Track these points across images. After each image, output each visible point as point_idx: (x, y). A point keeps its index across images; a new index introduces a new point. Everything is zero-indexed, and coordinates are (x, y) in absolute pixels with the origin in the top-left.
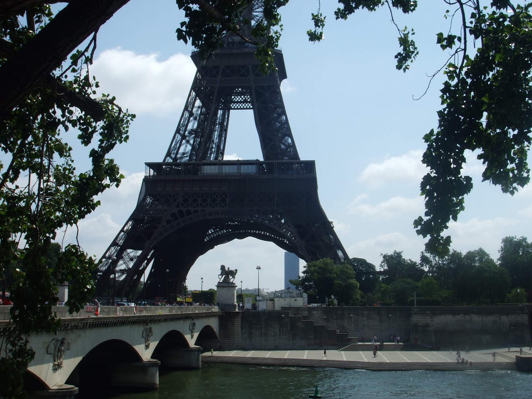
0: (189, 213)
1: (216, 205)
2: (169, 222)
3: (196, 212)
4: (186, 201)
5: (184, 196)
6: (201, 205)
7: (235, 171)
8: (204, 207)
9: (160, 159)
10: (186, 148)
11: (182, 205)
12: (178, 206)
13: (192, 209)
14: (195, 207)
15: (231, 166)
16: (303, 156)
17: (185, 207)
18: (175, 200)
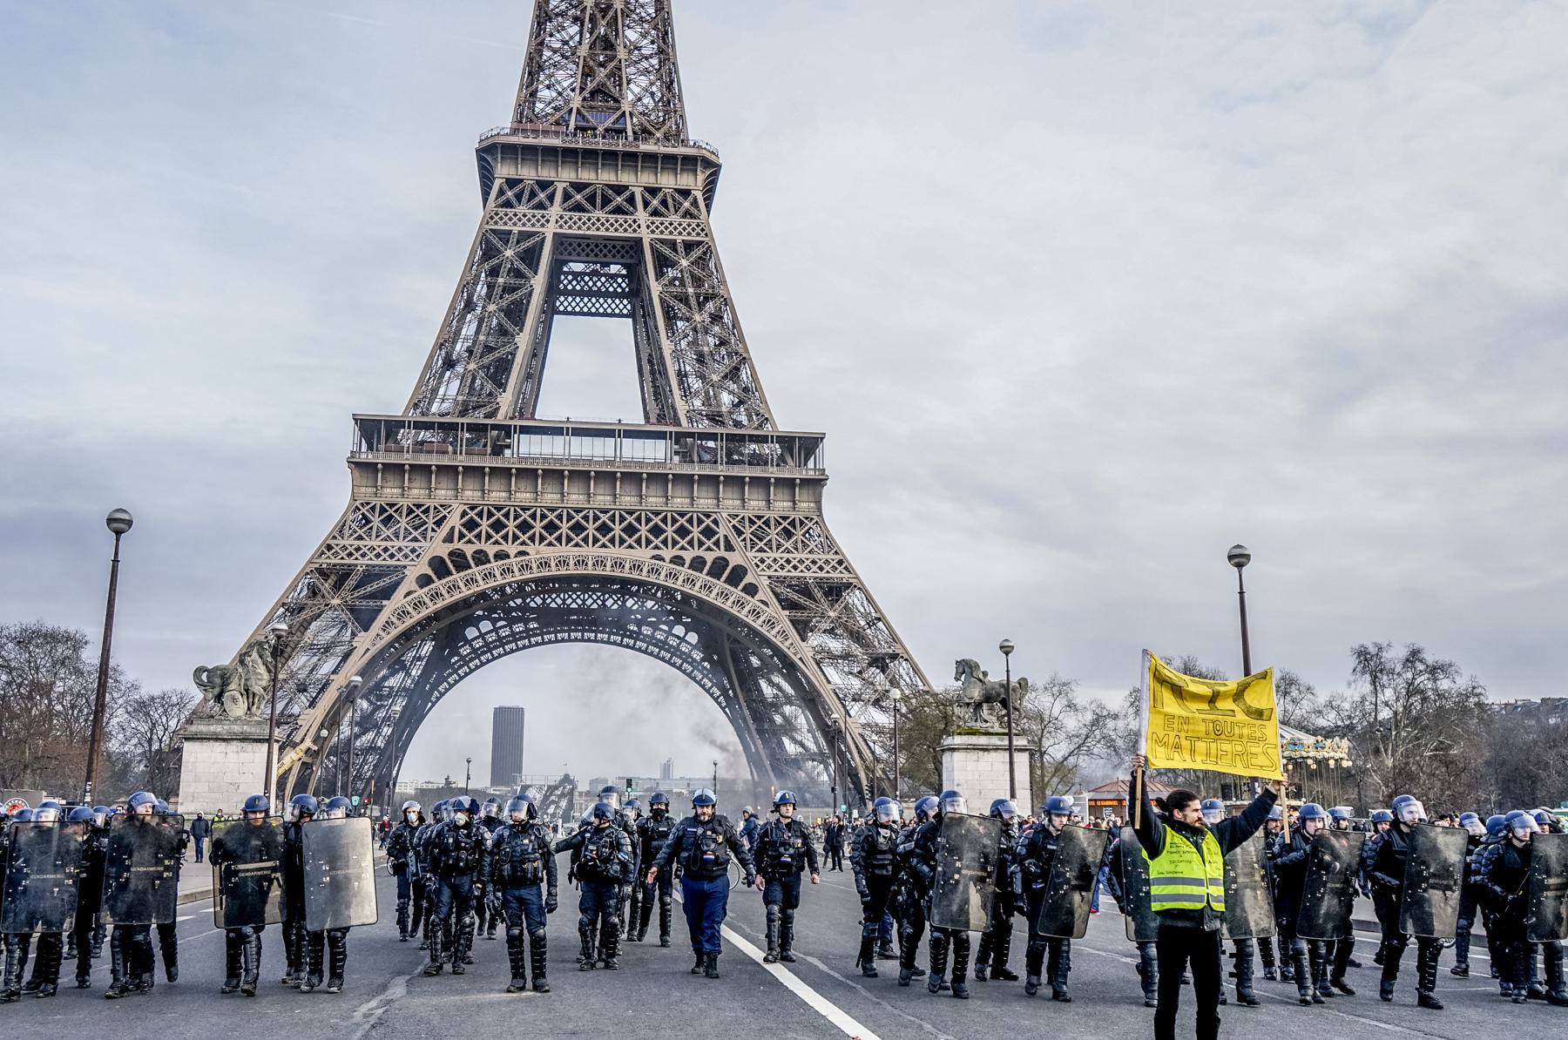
0: (481, 558)
1: (559, 539)
2: (424, 581)
3: (501, 556)
4: (471, 525)
5: (464, 514)
6: (516, 538)
7: (610, 453)
8: (523, 543)
9: (394, 401)
10: (451, 388)
11: (462, 536)
12: (449, 539)
13: (491, 550)
14: (497, 542)
15: (599, 441)
16: (786, 421)
17: (470, 541)
18: (439, 523)
